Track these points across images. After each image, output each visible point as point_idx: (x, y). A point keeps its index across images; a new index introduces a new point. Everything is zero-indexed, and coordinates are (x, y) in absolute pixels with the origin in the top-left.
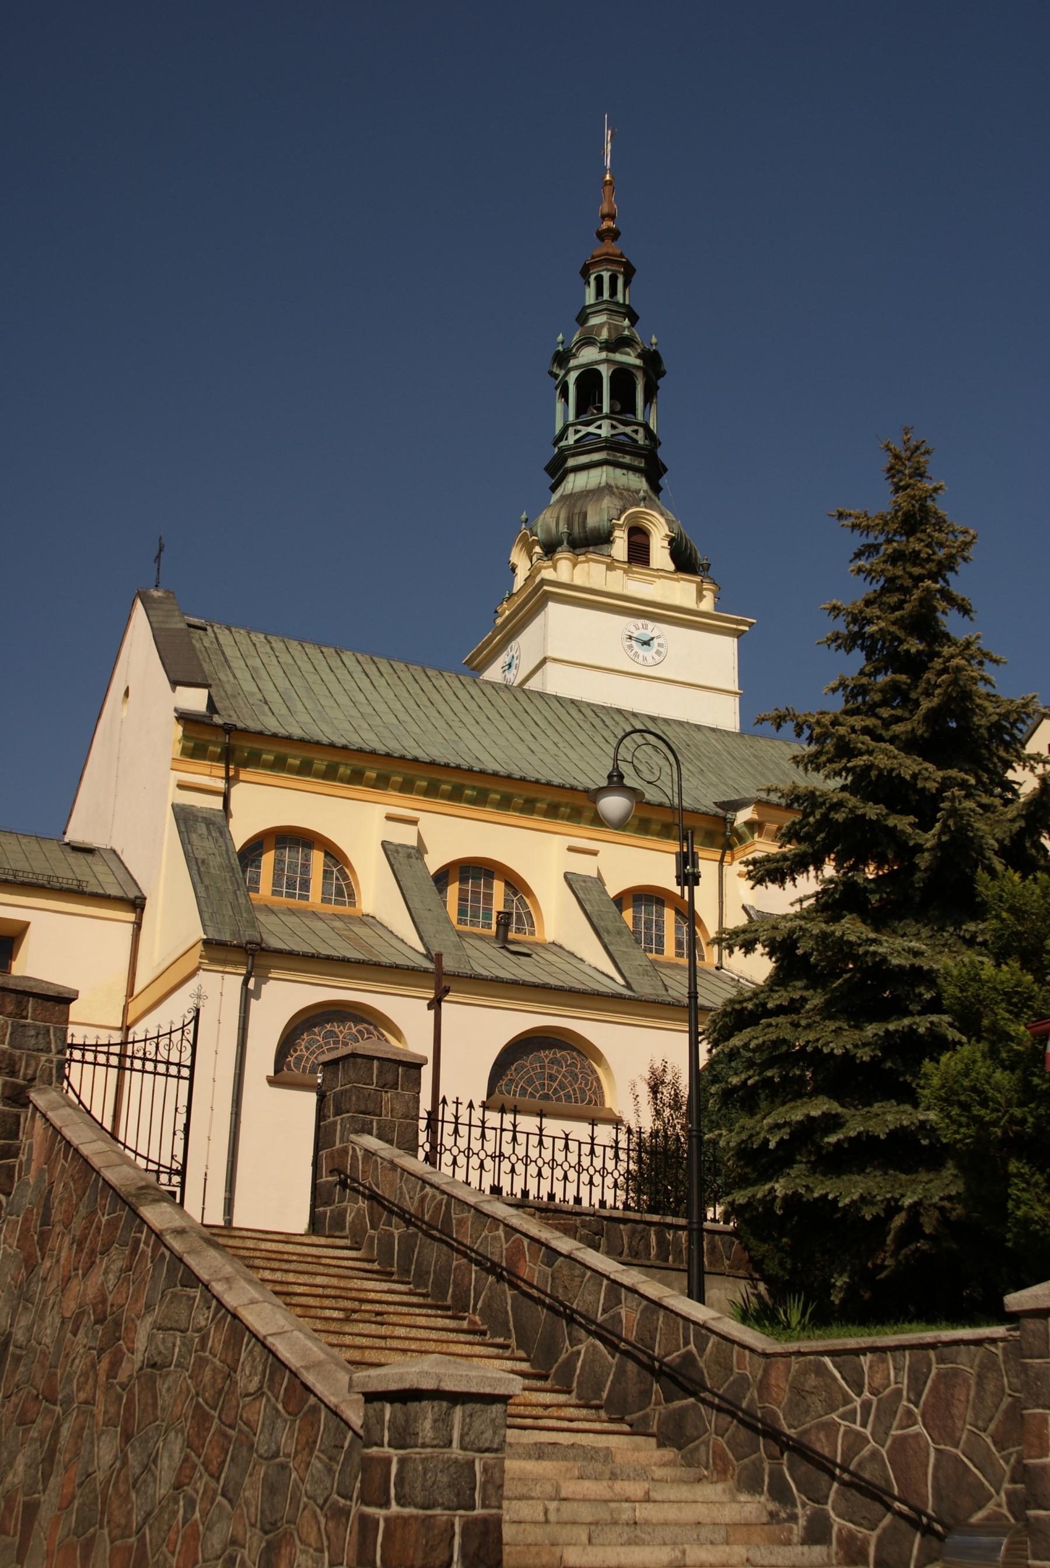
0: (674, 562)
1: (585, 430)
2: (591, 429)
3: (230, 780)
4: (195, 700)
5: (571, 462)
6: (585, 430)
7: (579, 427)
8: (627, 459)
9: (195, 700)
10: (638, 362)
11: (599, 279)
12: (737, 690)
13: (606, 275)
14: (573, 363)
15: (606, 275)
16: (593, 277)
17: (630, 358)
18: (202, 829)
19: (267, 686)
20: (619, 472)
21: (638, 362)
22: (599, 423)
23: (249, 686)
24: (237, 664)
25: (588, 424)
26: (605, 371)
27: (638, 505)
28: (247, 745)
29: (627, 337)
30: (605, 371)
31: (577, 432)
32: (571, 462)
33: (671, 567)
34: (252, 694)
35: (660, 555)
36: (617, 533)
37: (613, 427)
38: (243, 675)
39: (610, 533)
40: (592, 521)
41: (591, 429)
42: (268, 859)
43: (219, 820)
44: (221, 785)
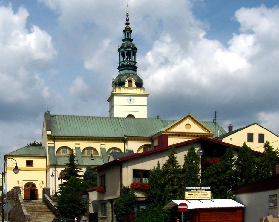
0: (136, 85)
3: (55, 142)
4: (49, 132)
8: (129, 68)
9: (49, 132)
10: (131, 50)
12: (147, 105)
13: (127, 33)
14: (120, 51)
17: (130, 49)
18: (51, 149)
19: (61, 126)
20: (128, 70)
21: (131, 50)
23: (59, 127)
24: (58, 122)
26: (125, 52)
27: (130, 77)
28: (56, 138)
29: (129, 46)
33: (135, 86)
34: (59, 128)
35: (134, 85)
36: (126, 82)
38: (58, 125)
39: (125, 82)
40: (122, 80)
42: (61, 150)
43: (53, 147)
44: (54, 143)
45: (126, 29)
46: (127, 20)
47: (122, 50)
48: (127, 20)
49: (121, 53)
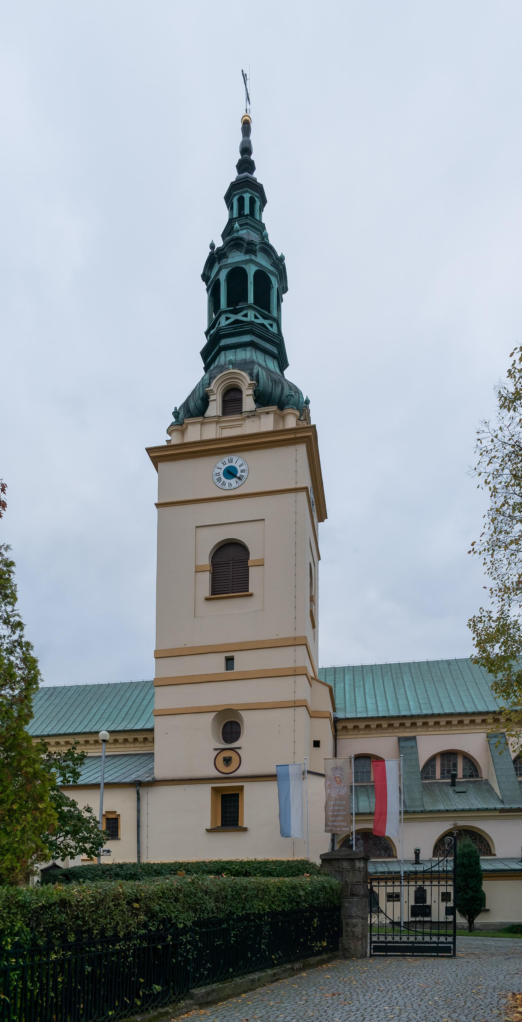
1: (233, 317)
2: (239, 317)
5: (223, 342)
6: (233, 317)
7: (229, 315)
11: (241, 201)
13: (247, 196)
15: (247, 196)
16: (237, 197)
22: (244, 312)
25: (236, 312)
30: (251, 270)
31: (227, 319)
32: (223, 342)
37: (256, 317)
41: (239, 317)
45: (238, 179)
46: (246, 150)
47: (236, 258)
48: (246, 150)
49: (223, 276)
